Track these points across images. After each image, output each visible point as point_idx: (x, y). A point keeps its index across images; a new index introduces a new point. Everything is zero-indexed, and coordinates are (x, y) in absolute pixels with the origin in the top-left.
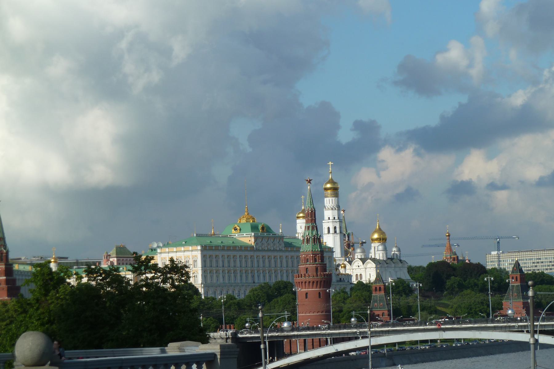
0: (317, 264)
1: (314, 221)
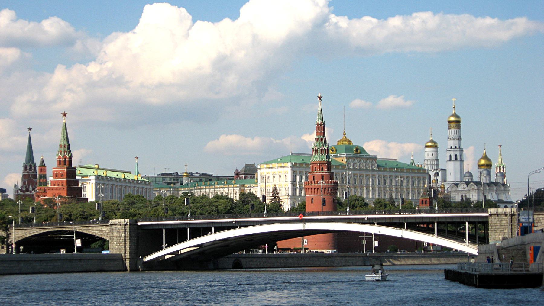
0: (323, 172)
1: (322, 134)
